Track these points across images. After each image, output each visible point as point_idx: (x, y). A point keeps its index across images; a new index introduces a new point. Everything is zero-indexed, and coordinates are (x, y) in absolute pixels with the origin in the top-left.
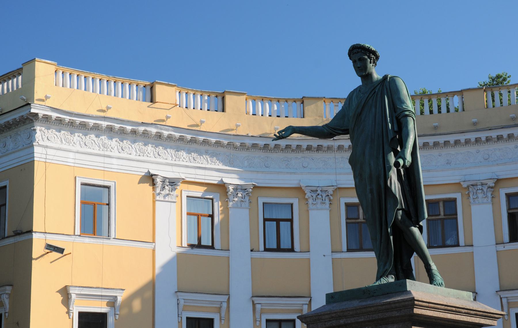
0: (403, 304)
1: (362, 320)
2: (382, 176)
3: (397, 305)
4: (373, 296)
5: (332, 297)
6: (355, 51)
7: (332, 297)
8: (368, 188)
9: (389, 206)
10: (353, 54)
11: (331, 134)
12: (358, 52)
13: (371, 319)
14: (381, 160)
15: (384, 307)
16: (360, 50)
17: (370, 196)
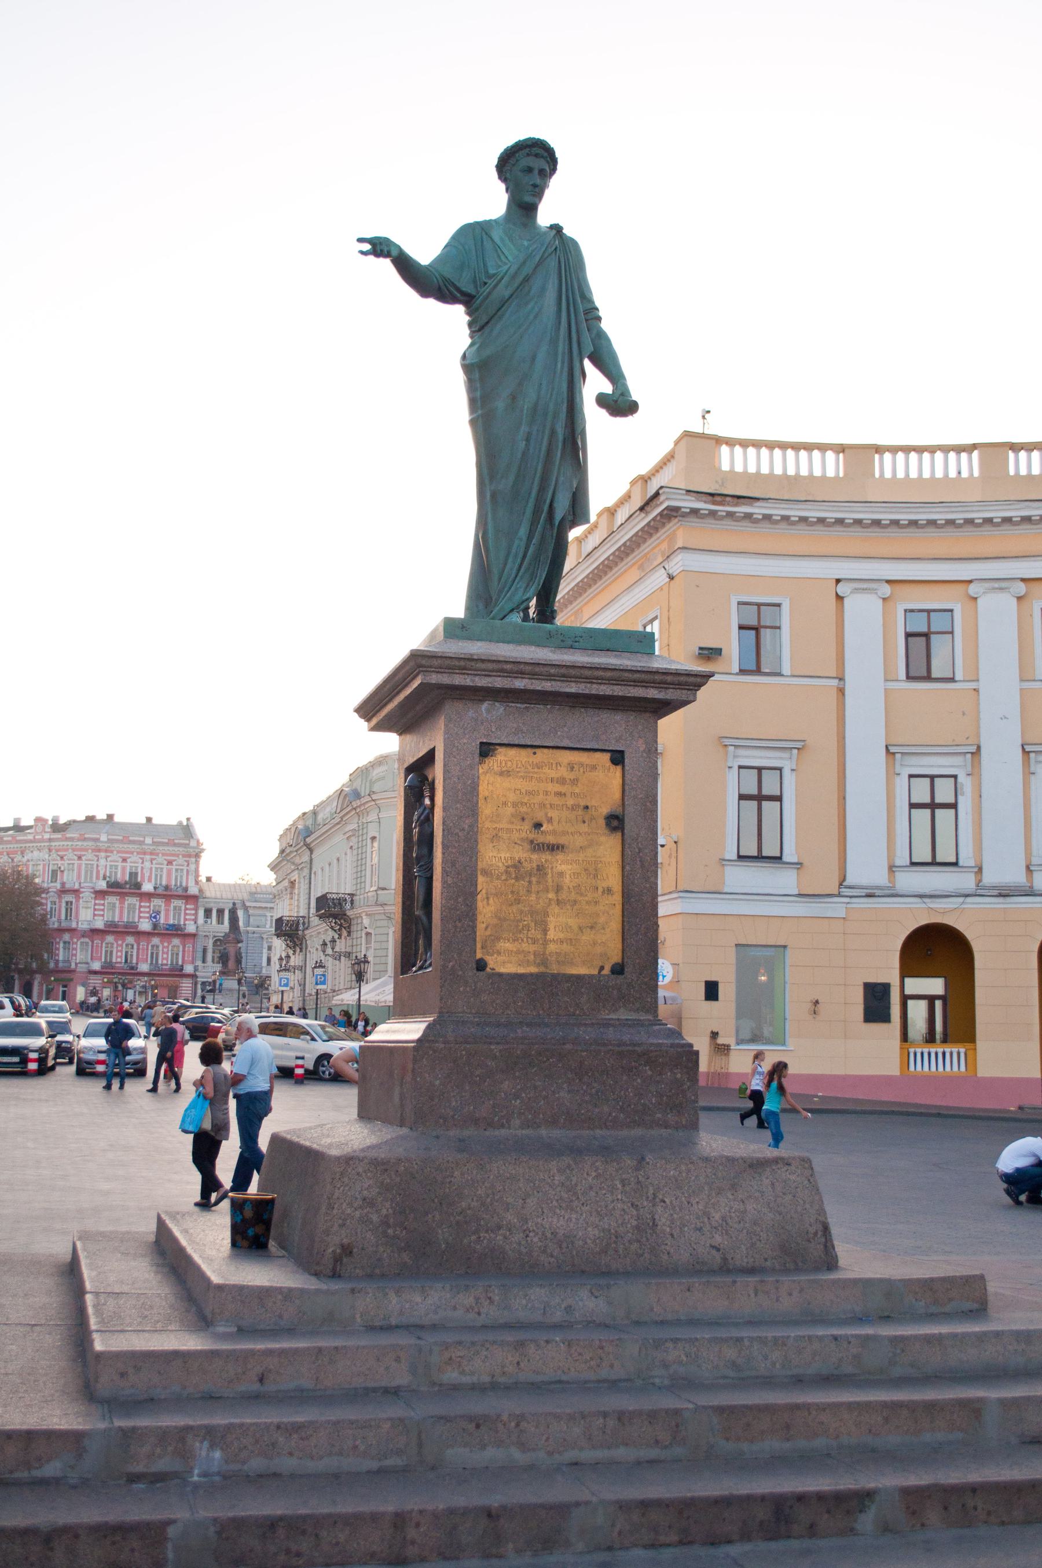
0: (682, 679)
1: (573, 690)
2: (563, 415)
3: (669, 678)
4: (571, 647)
5: (463, 627)
6: (535, 150)
7: (463, 627)
8: (524, 429)
9: (562, 479)
10: (528, 155)
11: (440, 289)
12: (542, 157)
13: (593, 692)
14: (565, 386)
15: (637, 676)
16: (546, 154)
17: (522, 445)
